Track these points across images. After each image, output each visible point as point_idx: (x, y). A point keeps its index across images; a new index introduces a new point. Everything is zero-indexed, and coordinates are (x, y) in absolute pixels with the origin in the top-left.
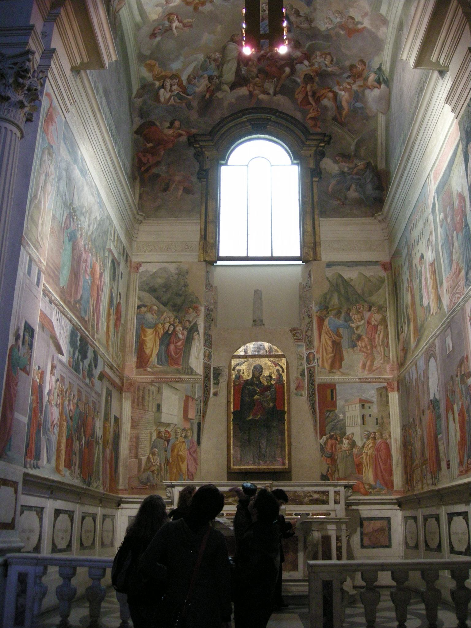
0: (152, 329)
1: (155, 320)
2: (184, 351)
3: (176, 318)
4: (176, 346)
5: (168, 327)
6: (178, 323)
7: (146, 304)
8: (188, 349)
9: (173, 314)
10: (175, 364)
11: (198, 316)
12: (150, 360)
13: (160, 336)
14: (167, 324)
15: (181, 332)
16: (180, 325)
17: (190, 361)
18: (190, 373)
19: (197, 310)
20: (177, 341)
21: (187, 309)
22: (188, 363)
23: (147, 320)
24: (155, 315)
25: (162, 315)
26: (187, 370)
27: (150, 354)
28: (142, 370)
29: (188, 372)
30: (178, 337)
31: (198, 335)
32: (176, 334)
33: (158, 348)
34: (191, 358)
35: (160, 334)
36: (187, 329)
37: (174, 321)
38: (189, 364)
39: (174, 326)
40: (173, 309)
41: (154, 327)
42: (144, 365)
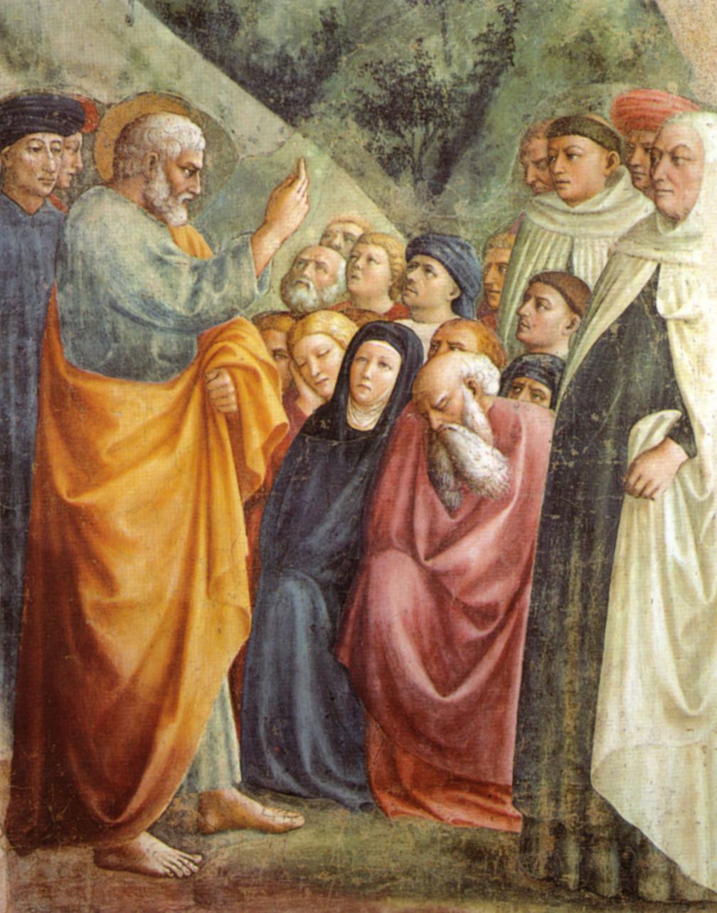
0: (164, 376)
1: (186, 282)
2: (531, 632)
3: (416, 248)
4: (436, 583)
5: (336, 357)
6: (444, 313)
7: (78, 87)
8: (574, 609)
9: (383, 203)
10: (454, 783)
11: (674, 220)
12: (166, 739)
13: (260, 467)
14: (320, 321)
15: (490, 415)
16: (468, 336)
17: (607, 743)
18: (611, 887)
19: (654, 154)
20: (445, 521)
21: (539, 146)
22: (584, 770)
23: (91, 281)
24: (179, 215)
25: (265, 223)
26: (573, 855)
27: (153, 673)
28: (74, 856)
29: (590, 878)
30: (459, 471)
31: (677, 452)
32: (435, 439)
33: (245, 602)
34: (609, 707)
35: (255, 440)
36: (551, 376)
37: (400, 285)
38: (597, 786)
39: (403, 341)
40: (388, 142)
41: (181, 361)
42: (94, 801)
